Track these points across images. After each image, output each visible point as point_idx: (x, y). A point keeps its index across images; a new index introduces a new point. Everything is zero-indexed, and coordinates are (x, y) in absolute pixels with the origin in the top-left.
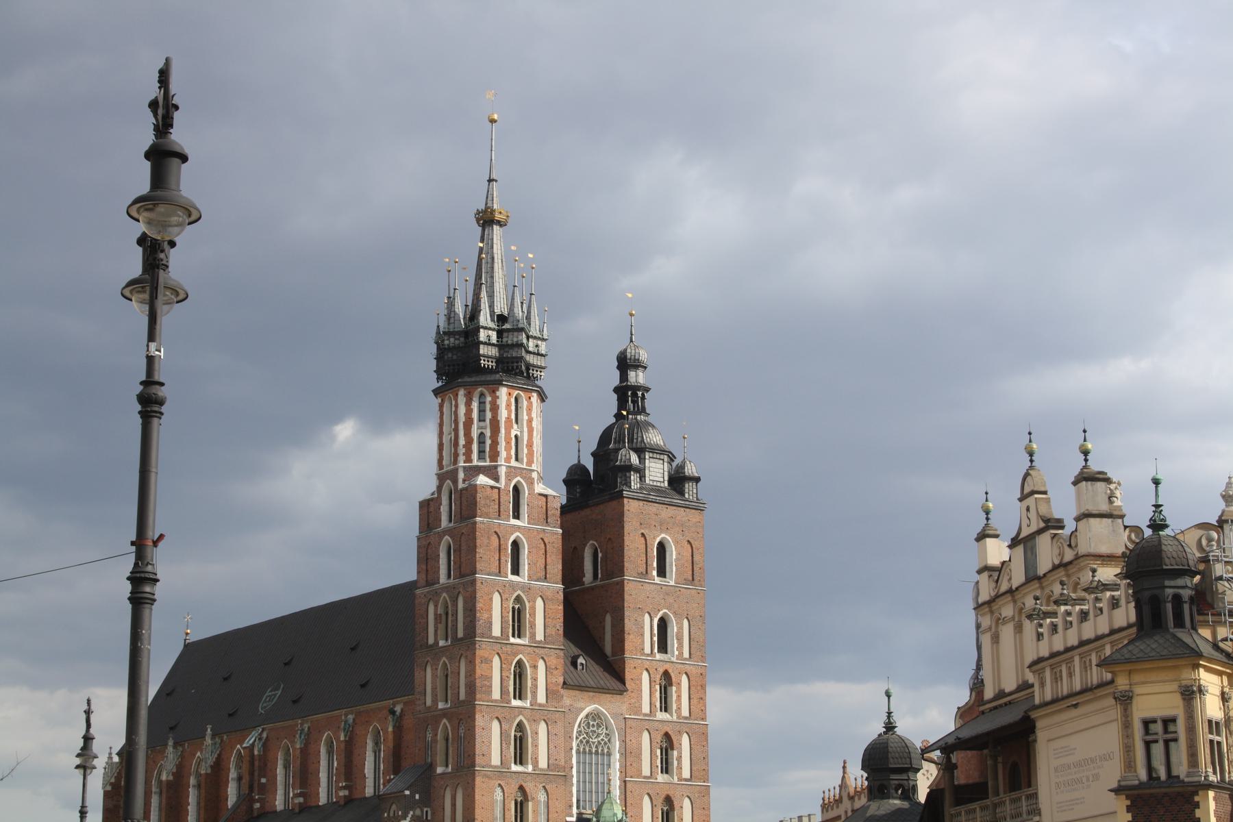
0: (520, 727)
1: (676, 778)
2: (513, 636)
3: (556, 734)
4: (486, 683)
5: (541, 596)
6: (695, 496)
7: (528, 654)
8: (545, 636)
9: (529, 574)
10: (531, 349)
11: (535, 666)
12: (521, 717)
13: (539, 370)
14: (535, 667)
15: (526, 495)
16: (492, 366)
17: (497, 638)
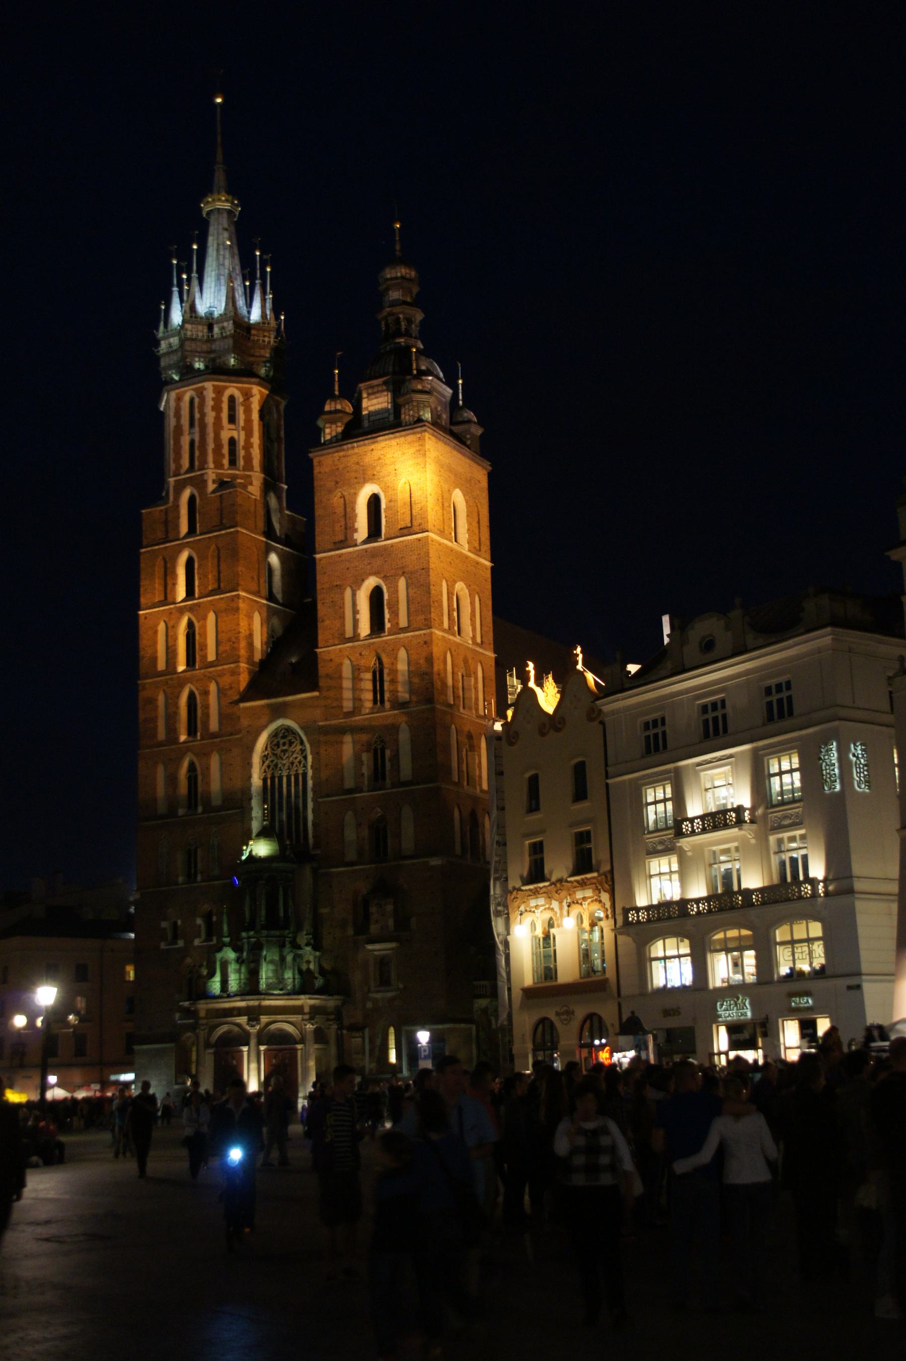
7: (197, 680)
14: (206, 693)
17: (162, 674)
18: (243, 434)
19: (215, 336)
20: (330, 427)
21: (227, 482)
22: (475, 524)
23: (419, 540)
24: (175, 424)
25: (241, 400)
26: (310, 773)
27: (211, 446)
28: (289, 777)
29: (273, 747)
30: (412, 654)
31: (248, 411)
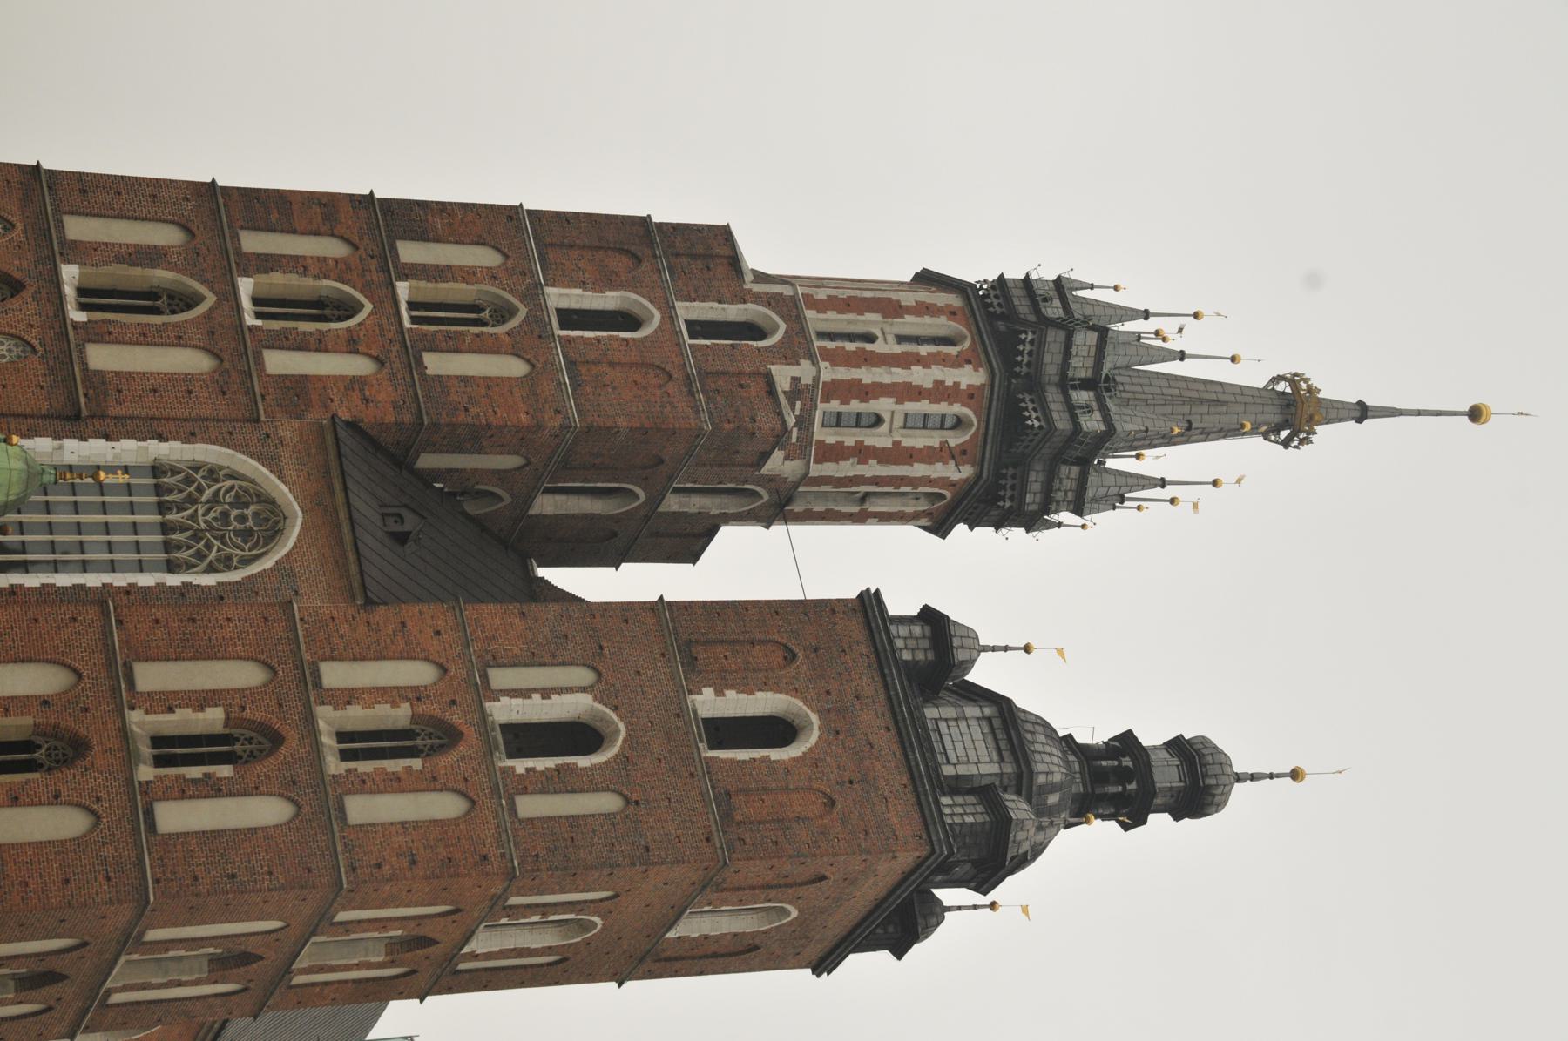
0: (187, 301)
1: (146, 772)
2: (412, 305)
3: (190, 392)
4: (274, 217)
5: (533, 366)
6: (957, 820)
7: (380, 325)
8: (439, 376)
9: (574, 339)
10: (1074, 395)
11: (354, 341)
12: (211, 299)
13: (1039, 414)
14: (351, 345)
15: (754, 344)
16: (991, 305)
18: (886, 443)
19: (1074, 395)
20: (924, 637)
21: (793, 410)
22: (713, 948)
23: (708, 840)
24: (903, 303)
25: (953, 443)
26: (174, 580)
27: (867, 375)
28: (165, 528)
29: (233, 493)
30: (457, 825)
31: (929, 456)
